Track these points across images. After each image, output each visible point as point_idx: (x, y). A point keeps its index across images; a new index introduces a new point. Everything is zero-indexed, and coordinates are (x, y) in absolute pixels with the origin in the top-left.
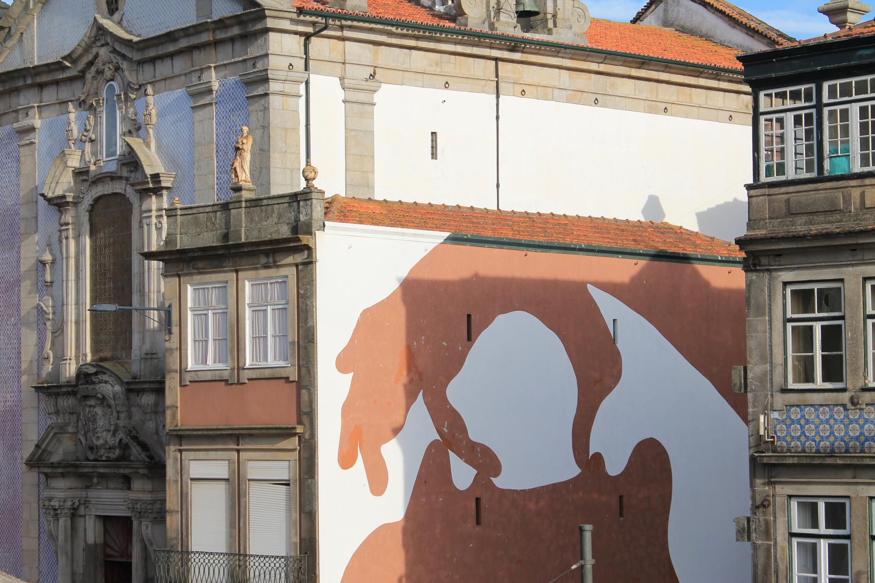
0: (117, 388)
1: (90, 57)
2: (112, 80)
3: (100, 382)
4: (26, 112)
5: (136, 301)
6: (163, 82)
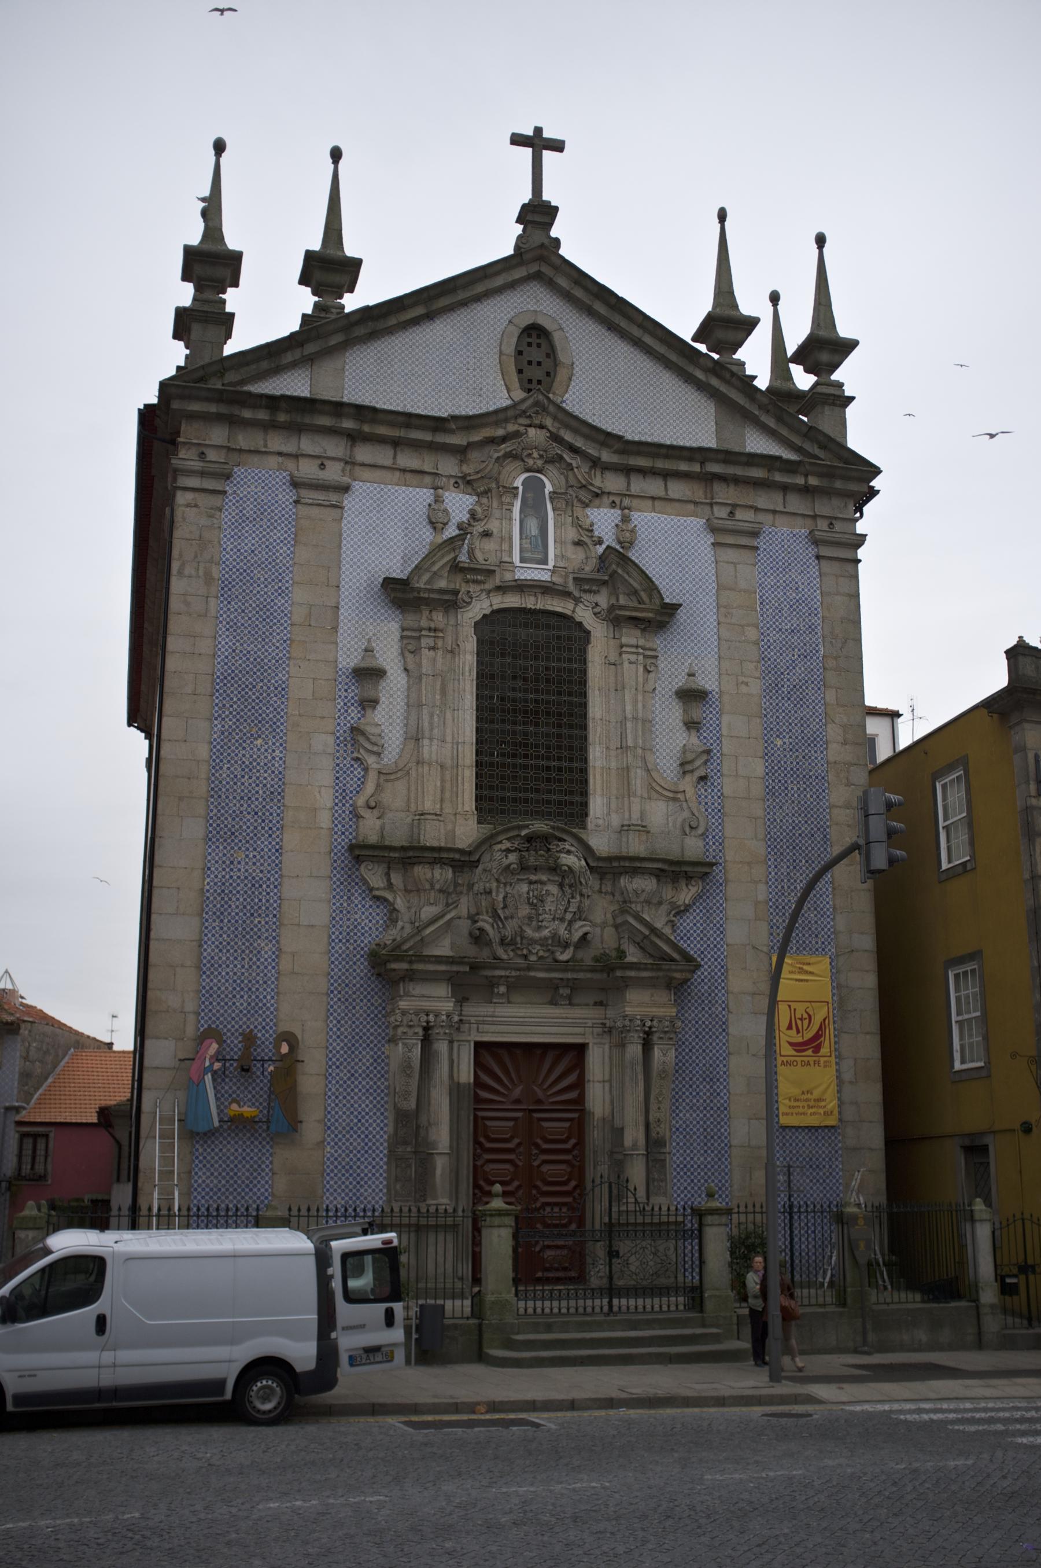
0: (583, 863)
1: (500, 432)
2: (539, 471)
3: (560, 852)
5: (598, 754)
6: (649, 503)
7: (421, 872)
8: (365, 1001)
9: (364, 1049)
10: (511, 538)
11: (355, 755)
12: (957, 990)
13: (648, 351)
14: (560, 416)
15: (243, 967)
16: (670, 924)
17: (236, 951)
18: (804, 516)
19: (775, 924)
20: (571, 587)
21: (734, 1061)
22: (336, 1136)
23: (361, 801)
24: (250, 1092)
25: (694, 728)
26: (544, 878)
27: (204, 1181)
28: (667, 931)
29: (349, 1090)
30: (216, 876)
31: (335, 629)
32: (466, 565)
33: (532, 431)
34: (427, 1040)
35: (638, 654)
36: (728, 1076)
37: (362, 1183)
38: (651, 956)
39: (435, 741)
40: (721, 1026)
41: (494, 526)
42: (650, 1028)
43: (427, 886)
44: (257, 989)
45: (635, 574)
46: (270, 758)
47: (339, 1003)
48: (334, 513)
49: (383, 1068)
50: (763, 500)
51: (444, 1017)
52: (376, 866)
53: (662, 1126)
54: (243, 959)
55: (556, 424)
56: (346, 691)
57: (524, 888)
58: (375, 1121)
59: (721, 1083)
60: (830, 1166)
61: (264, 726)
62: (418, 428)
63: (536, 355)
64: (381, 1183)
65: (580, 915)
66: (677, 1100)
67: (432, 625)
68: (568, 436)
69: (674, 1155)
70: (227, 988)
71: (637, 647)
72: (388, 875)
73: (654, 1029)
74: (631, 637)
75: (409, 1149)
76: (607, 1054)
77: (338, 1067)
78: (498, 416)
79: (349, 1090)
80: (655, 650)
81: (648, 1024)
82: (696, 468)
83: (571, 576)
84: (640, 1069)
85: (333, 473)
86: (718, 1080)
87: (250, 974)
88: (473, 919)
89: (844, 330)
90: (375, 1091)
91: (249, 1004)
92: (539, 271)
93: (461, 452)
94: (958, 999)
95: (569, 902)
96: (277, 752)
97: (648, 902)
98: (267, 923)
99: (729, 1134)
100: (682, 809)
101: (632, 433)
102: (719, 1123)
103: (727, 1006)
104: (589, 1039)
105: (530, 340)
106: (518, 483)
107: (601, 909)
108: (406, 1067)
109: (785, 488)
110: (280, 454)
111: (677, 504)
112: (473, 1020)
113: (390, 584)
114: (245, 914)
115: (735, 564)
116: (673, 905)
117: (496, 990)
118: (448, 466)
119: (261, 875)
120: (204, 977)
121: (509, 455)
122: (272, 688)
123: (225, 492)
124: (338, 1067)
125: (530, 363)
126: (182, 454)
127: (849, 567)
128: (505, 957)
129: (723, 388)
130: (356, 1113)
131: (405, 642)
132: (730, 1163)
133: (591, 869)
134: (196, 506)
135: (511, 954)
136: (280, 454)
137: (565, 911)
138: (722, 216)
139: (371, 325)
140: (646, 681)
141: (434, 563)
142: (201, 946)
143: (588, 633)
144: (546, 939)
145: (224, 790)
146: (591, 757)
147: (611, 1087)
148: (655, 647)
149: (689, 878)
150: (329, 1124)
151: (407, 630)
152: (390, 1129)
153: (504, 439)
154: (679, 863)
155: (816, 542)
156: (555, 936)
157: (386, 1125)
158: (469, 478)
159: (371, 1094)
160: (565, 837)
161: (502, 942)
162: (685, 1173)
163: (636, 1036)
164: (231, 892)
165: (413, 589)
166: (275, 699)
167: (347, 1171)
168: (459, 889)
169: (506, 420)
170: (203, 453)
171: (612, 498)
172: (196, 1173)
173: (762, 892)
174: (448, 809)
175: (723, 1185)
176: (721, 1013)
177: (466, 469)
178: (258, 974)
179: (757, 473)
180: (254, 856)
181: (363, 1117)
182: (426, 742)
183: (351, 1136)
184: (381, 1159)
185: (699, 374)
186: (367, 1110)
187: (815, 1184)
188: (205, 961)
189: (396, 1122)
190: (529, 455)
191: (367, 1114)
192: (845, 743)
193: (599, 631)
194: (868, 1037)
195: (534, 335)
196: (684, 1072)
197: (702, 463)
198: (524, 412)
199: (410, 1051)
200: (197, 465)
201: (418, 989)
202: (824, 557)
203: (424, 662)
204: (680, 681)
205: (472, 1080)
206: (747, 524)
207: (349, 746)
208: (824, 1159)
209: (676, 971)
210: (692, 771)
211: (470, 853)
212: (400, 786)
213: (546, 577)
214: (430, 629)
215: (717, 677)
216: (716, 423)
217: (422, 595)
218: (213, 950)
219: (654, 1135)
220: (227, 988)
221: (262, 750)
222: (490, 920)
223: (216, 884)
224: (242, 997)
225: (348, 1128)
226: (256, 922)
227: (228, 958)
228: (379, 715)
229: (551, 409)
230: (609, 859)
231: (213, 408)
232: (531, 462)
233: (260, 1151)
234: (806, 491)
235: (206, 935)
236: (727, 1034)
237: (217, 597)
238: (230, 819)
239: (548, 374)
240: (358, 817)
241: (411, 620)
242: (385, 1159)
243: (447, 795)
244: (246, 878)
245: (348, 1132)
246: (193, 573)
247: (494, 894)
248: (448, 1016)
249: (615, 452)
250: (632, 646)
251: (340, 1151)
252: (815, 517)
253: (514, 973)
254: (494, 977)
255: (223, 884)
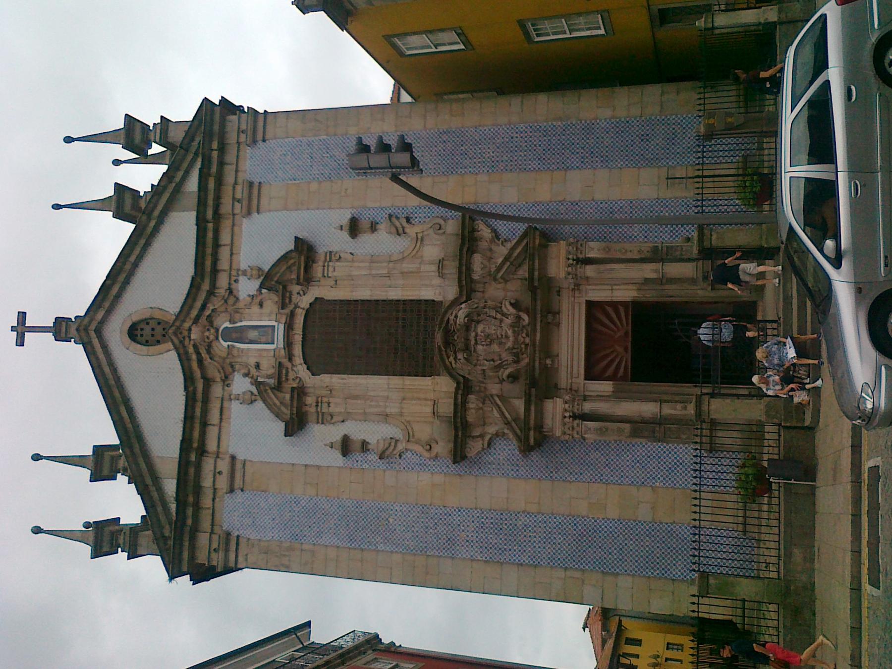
0: (463, 306)
1: (194, 357)
2: (217, 330)
3: (456, 323)
4: (218, 475)
5: (393, 293)
6: (234, 257)
7: (471, 417)
8: (557, 455)
9: (589, 457)
10: (259, 350)
11: (397, 456)
12: (548, 34)
13: (140, 257)
14: (182, 318)
15: (535, 537)
16: (505, 244)
17: (525, 541)
18: (238, 151)
19: (504, 168)
20: (287, 311)
21: (598, 196)
22: (648, 478)
23: (427, 454)
24: (618, 536)
25: (375, 226)
26: (473, 334)
27: (679, 571)
28: (509, 245)
29: (617, 468)
30: (477, 552)
31: (318, 467)
32: (276, 381)
33: (193, 336)
34: (585, 417)
35: (328, 266)
36: (609, 200)
37: (681, 461)
38: (525, 259)
39: (387, 404)
40: (574, 206)
41: (252, 361)
42: (574, 260)
43: (481, 411)
44: (550, 528)
45: (277, 269)
46: (400, 513)
47: (559, 473)
48: (248, 466)
49: (603, 444)
50: (229, 178)
51: (567, 406)
52: (469, 446)
53: (643, 249)
54: (530, 536)
55: (188, 320)
56: (357, 461)
57: (480, 347)
58: (638, 451)
59: (614, 205)
60: (674, 124)
61: (381, 516)
62: (194, 412)
63: (147, 330)
64: (681, 448)
65: (498, 309)
66: (625, 237)
67: (314, 404)
68: (194, 313)
69: (664, 239)
70: (549, 548)
71: (324, 266)
72: (474, 437)
73: (575, 257)
74: (318, 270)
75: (658, 429)
76: (594, 287)
77: (602, 475)
78: (184, 358)
79: (617, 468)
80: (326, 253)
81: (571, 261)
82: (210, 226)
83: (281, 311)
84: (602, 267)
85: (223, 465)
86: (611, 208)
87: (540, 532)
88: (502, 381)
89: (119, 124)
90: (618, 450)
91: (560, 533)
92: (95, 330)
93: (208, 382)
94: (555, 34)
95: (489, 316)
96: (397, 508)
97: (490, 259)
98: (506, 519)
99: (649, 200)
100: (428, 235)
101: (191, 271)
102: (642, 207)
103: (560, 202)
104: (583, 301)
105: (139, 335)
106: (225, 344)
107: (494, 291)
108: (601, 431)
109: (222, 164)
110: (214, 500)
111: (235, 237)
112: (570, 381)
113: (288, 433)
114: (501, 534)
115: (270, 198)
116: (492, 241)
117: (549, 366)
118: (217, 390)
119: (475, 522)
120: (542, 563)
121: (209, 352)
122: (357, 510)
123: (238, 537)
124: (602, 475)
125: (153, 335)
126: (214, 563)
127: (270, 119)
128: (526, 361)
129: (160, 207)
130: (633, 464)
131: (325, 422)
132: (670, 199)
133: (469, 298)
134: (247, 555)
135: (525, 356)
136: (214, 500)
137: (495, 318)
138: (57, 207)
139: (134, 440)
140: (346, 261)
141: (275, 404)
142: (521, 564)
143: (316, 299)
144: (514, 332)
145: (421, 544)
146: (395, 298)
147: (615, 285)
148: (324, 254)
149: (473, 230)
150: (640, 483)
151: (318, 419)
152: (644, 441)
153: (198, 354)
154: (463, 239)
155: (255, 142)
156: (512, 326)
157: (641, 443)
158: (223, 378)
159: (620, 453)
160: (446, 319)
161: (517, 362)
162: (677, 231)
163: (579, 270)
164: (486, 543)
165: (291, 418)
166: (363, 508)
167: (673, 471)
168: (482, 389)
169: (187, 353)
170: (215, 550)
171: (233, 282)
172: (674, 575)
173: (483, 178)
174: (431, 396)
175: (686, 204)
176: (565, 206)
177: (218, 379)
178: (540, 527)
179: (211, 184)
180: (464, 526)
181: (636, 459)
182: (388, 410)
183: (649, 467)
184: (665, 447)
185: (152, 223)
186: (631, 456)
187: (686, 136)
188: (532, 562)
189: (639, 437)
190: (208, 338)
191: (633, 456)
192: (383, 120)
193: (315, 292)
194: (582, 98)
195: (136, 332)
196: (605, 232)
197: (208, 222)
198: (181, 342)
199: (590, 429)
200: (221, 554)
201: (548, 422)
202: (264, 137)
203: (337, 410)
204: (345, 235)
205: (611, 382)
206: (245, 189)
207: (392, 460)
208: (669, 129)
209: (534, 243)
210: (403, 228)
211: (458, 383)
212: (416, 427)
213: (282, 327)
214: (317, 406)
215: (342, 210)
216: (184, 211)
217: (295, 412)
218: (525, 556)
219: (648, 255)
220: (549, 548)
221: (396, 518)
222: (502, 370)
223: (481, 552)
224: (555, 538)
225: (643, 470)
226: (506, 527)
227: (529, 546)
228: (372, 440)
229: (177, 324)
230: (460, 286)
231: (186, 544)
232: (212, 337)
233: (658, 531)
234: (222, 149)
235: (515, 560)
236: (580, 201)
237: (302, 543)
238: (440, 541)
239: (159, 323)
240: (436, 457)
241: (312, 417)
242: (665, 444)
243: (422, 396)
244: (477, 532)
245: (646, 470)
246: (287, 558)
247: (484, 368)
248: (566, 403)
249: (203, 279)
250: (324, 269)
251: (659, 476)
252: (239, 143)
253: (537, 355)
254: (540, 368)
255: (481, 547)
